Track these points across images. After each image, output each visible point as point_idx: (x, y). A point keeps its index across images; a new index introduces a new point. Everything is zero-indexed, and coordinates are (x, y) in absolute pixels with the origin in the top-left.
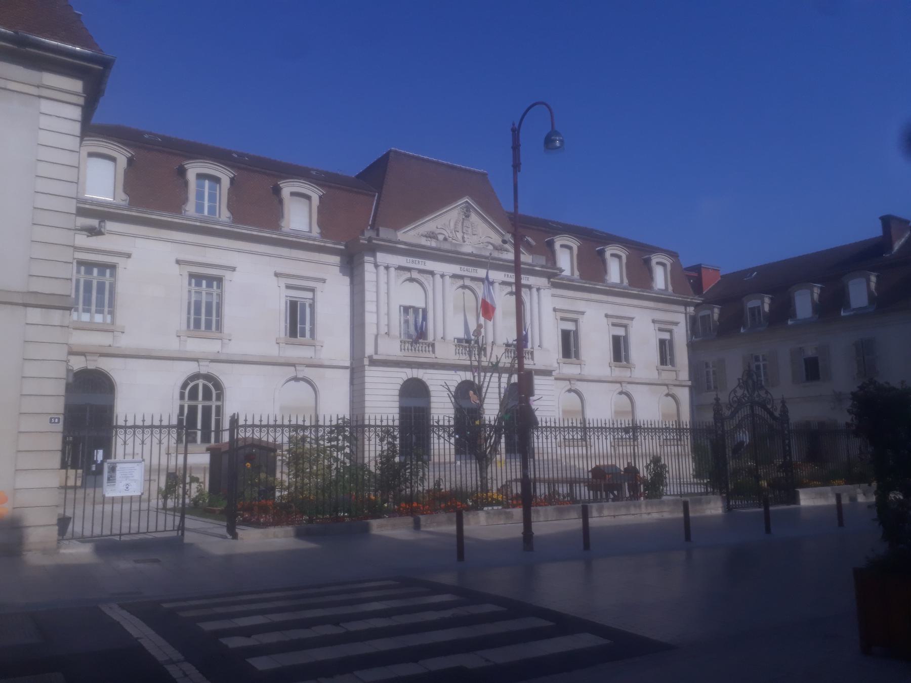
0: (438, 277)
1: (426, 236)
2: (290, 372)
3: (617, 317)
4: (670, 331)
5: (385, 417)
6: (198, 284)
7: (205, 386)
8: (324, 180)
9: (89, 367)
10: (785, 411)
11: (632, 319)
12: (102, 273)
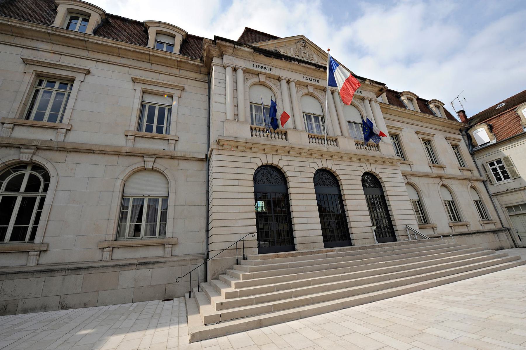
0: (284, 83)
2: (138, 163)
7: (31, 176)
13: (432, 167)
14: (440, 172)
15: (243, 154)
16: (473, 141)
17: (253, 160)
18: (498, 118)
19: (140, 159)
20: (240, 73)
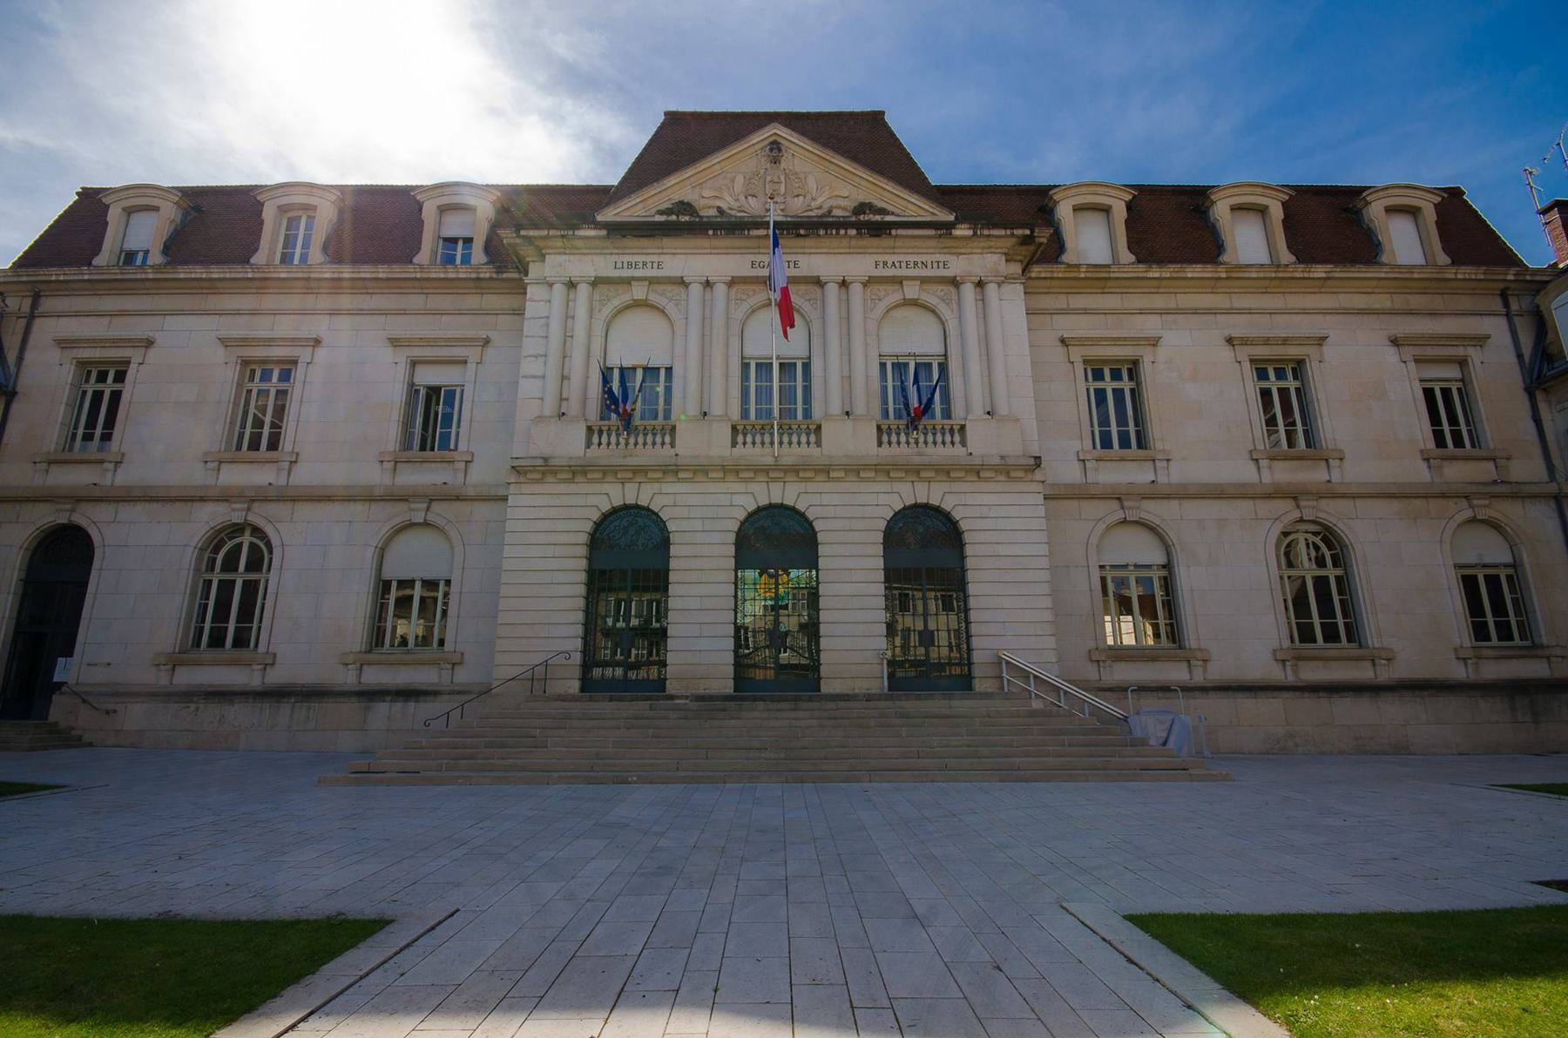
2: (400, 513)
3: (1267, 341)
4: (1462, 363)
7: (252, 544)
11: (1321, 341)
13: (1264, 463)
14: (1314, 475)
15: (573, 488)
16: (1550, 336)
17: (592, 500)
19: (403, 506)
20: (583, 290)
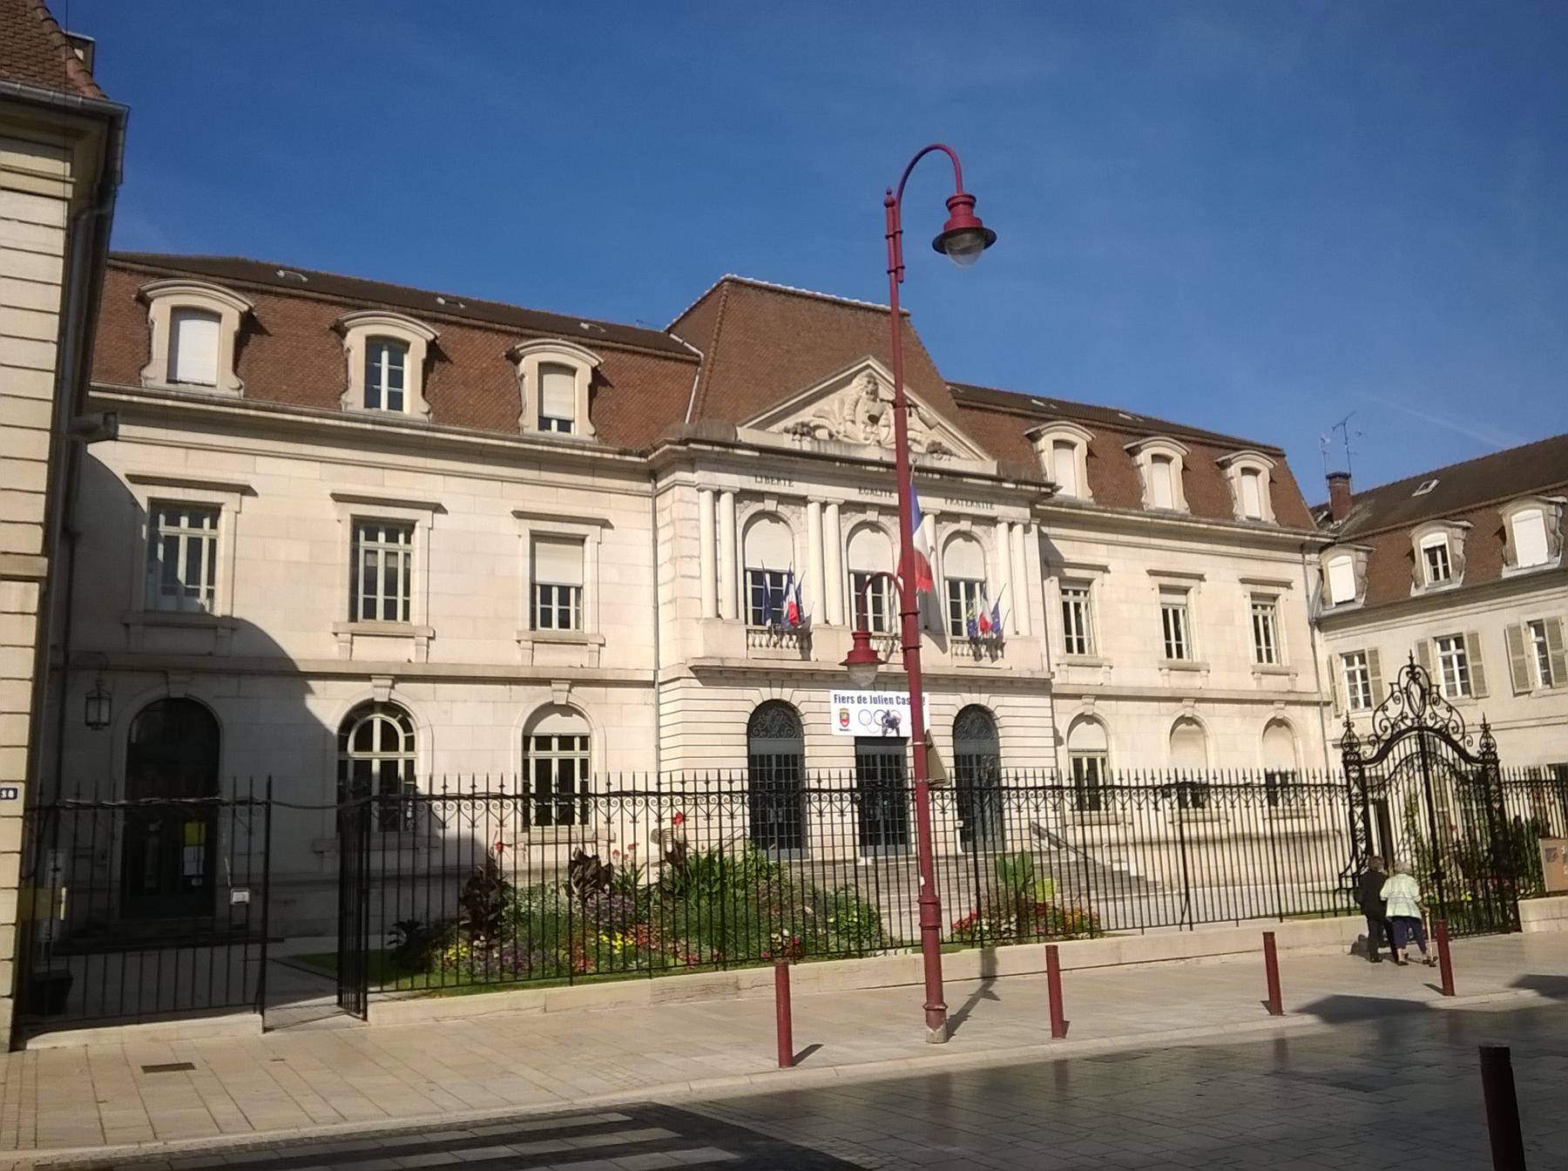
1: (787, 431)
5: (689, 776)
6: (372, 537)
7: (385, 724)
8: (597, 338)
9: (174, 695)
10: (1489, 749)
12: (196, 523)
18: (1388, 536)
